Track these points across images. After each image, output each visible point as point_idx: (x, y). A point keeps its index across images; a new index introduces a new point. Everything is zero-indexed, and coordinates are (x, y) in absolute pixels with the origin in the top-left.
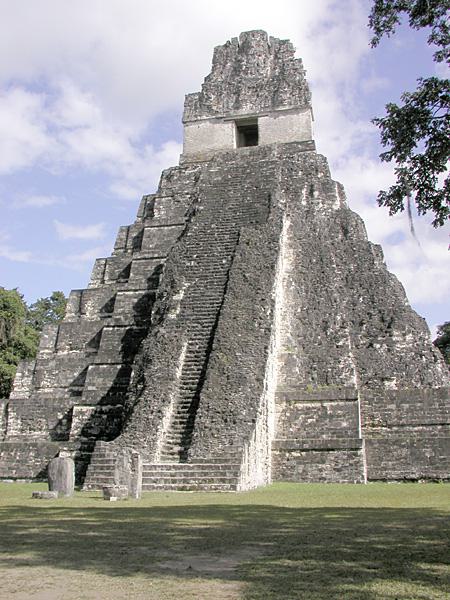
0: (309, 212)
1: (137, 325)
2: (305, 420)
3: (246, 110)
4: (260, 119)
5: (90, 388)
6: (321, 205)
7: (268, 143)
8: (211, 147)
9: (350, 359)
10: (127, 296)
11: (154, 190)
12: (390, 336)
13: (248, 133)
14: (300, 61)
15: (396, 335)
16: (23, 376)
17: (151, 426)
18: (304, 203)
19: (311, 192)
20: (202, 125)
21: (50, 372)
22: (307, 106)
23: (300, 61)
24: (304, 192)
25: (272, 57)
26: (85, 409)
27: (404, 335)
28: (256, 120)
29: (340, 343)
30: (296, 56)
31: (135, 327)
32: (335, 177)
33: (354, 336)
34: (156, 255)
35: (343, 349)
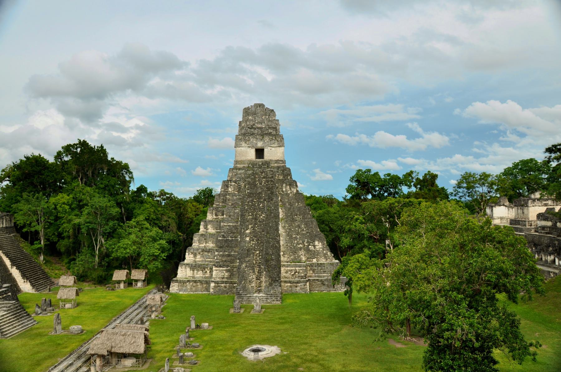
0: (287, 195)
3: (260, 145)
4: (265, 150)
9: (302, 252)
13: (260, 153)
14: (278, 120)
21: (199, 253)
24: (284, 185)
26: (217, 269)
28: (263, 149)
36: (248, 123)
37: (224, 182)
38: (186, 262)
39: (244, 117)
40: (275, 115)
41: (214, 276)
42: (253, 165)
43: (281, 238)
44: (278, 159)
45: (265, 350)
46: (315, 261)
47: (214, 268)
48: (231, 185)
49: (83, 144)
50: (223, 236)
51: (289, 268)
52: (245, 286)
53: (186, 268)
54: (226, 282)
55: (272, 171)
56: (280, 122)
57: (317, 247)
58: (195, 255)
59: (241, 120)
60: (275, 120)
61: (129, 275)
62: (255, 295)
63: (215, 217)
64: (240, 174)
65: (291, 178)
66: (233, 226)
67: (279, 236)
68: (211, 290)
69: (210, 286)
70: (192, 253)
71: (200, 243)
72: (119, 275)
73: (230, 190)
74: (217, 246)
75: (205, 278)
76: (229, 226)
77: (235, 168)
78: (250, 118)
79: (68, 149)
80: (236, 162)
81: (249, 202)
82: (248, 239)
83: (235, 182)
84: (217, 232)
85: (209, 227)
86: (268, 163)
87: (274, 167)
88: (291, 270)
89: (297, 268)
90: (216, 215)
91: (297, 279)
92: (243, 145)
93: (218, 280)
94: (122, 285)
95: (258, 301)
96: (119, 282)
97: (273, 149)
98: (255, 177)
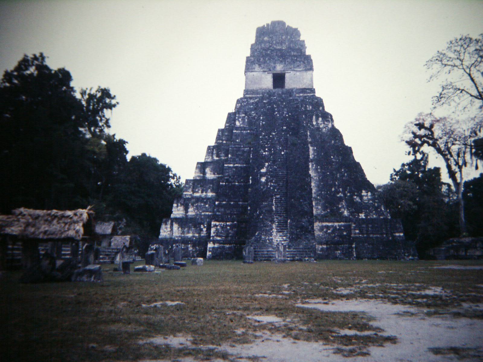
0: (318, 129)
1: (238, 183)
2: (326, 232)
3: (279, 68)
4: (287, 75)
5: (218, 213)
6: (323, 125)
7: (290, 87)
8: (260, 87)
10: (230, 167)
11: (232, 110)
12: (362, 192)
14: (304, 41)
15: (364, 193)
16: (177, 206)
20: (254, 73)
21: (193, 205)
22: (311, 69)
23: (304, 41)
24: (314, 117)
25: (289, 37)
26: (217, 223)
27: (367, 192)
29: (338, 196)
30: (302, 38)
31: (237, 184)
32: (327, 109)
34: (242, 146)
36: (263, 45)
37: (230, 114)
38: (172, 216)
39: (257, 37)
41: (212, 234)
42: (270, 94)
44: (304, 87)
46: (362, 216)
48: (239, 117)
50: (227, 181)
52: (260, 238)
53: (172, 225)
56: (307, 44)
57: (365, 198)
60: (299, 40)
63: (216, 158)
66: (241, 167)
68: (209, 254)
70: (182, 205)
71: (194, 192)
75: (200, 237)
78: (266, 39)
81: (264, 136)
82: (263, 180)
83: (246, 114)
84: (218, 178)
88: (328, 227)
89: (336, 224)
90: (218, 156)
92: (256, 70)
93: (219, 238)
97: (298, 73)
98: (273, 108)
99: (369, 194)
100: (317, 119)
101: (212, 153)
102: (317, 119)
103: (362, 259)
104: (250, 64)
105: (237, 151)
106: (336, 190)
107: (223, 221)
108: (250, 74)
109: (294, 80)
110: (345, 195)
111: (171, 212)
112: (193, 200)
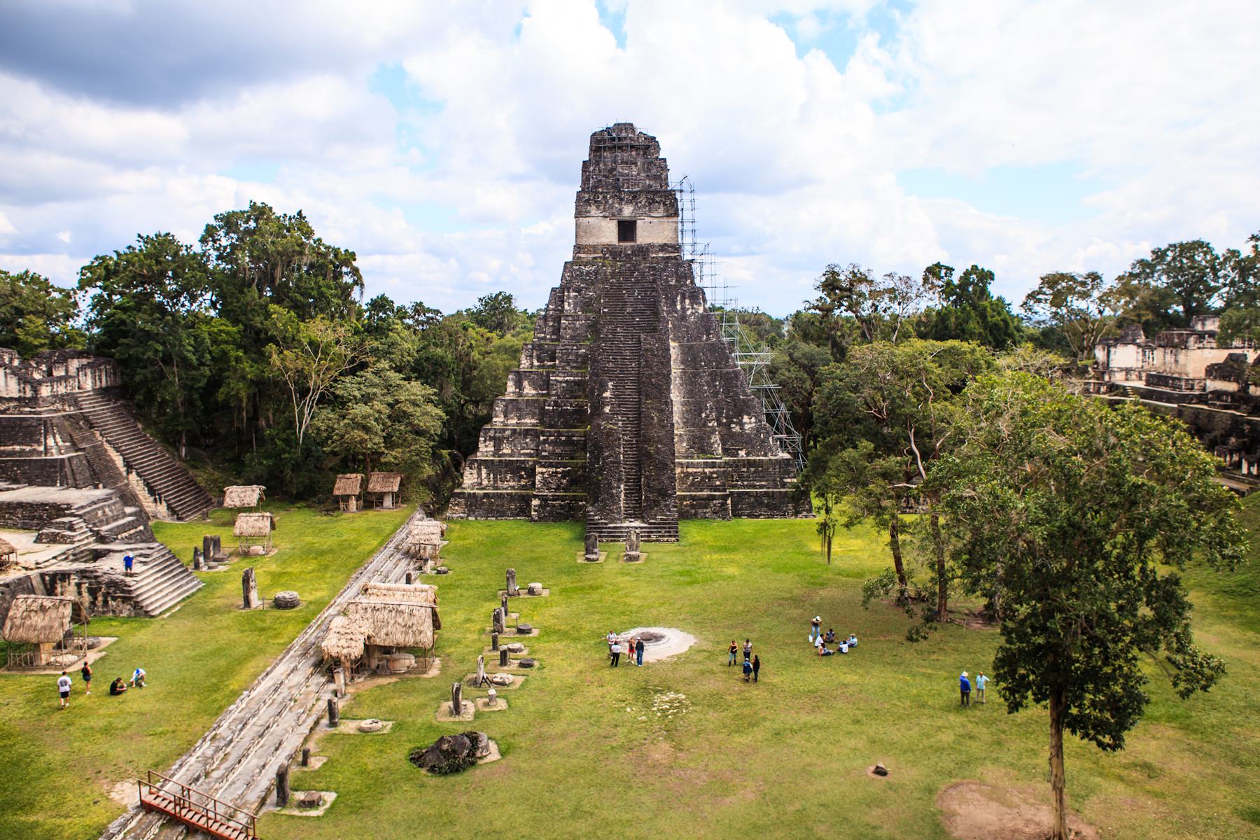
0: (683, 317)
3: (628, 211)
9: (716, 438)
13: (627, 229)
14: (665, 160)
15: (746, 419)
17: (614, 499)
18: (679, 307)
19: (683, 299)
23: (665, 160)
33: (718, 420)
35: (713, 432)
37: (553, 290)
38: (479, 456)
40: (657, 147)
43: (675, 409)
45: (662, 637)
47: (538, 469)
48: (569, 297)
49: (260, 212)
51: (690, 470)
53: (480, 470)
54: (562, 498)
55: (654, 268)
57: (747, 427)
58: (498, 442)
59: (587, 159)
61: (365, 483)
62: (626, 524)
63: (536, 363)
64: (588, 273)
65: (693, 282)
67: (669, 403)
69: (529, 505)
70: (491, 439)
72: (348, 484)
73: (566, 307)
74: (541, 422)
76: (566, 382)
77: (577, 260)
79: (229, 221)
80: (578, 248)
82: (607, 409)
83: (578, 290)
85: (526, 383)
86: (644, 251)
87: (658, 260)
91: (705, 493)
94: (353, 503)
95: (634, 538)
96: (346, 498)
99: (753, 420)
100: (683, 301)
101: (531, 356)
102: (683, 301)
103: (740, 516)
104: (584, 203)
105: (569, 354)
106: (707, 416)
107: (551, 465)
108: (583, 221)
109: (651, 231)
110: (720, 424)
111: (477, 448)
112: (508, 433)
